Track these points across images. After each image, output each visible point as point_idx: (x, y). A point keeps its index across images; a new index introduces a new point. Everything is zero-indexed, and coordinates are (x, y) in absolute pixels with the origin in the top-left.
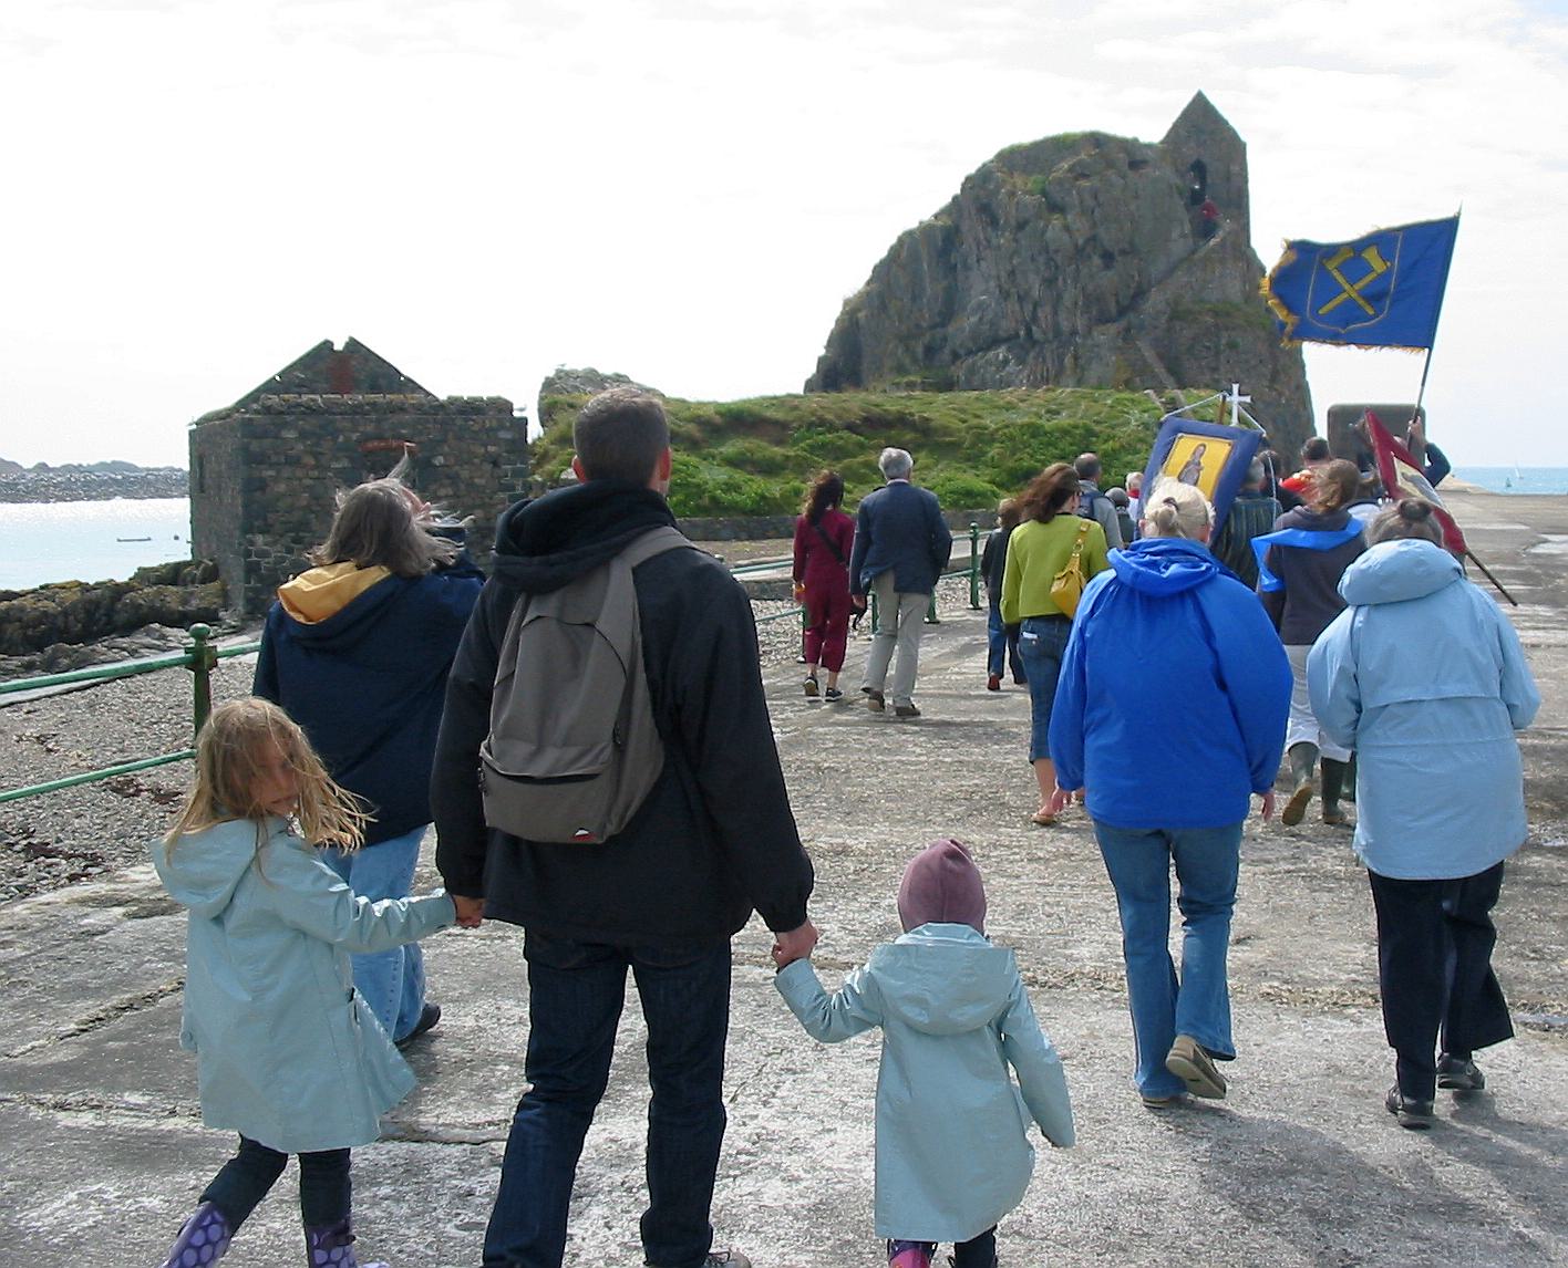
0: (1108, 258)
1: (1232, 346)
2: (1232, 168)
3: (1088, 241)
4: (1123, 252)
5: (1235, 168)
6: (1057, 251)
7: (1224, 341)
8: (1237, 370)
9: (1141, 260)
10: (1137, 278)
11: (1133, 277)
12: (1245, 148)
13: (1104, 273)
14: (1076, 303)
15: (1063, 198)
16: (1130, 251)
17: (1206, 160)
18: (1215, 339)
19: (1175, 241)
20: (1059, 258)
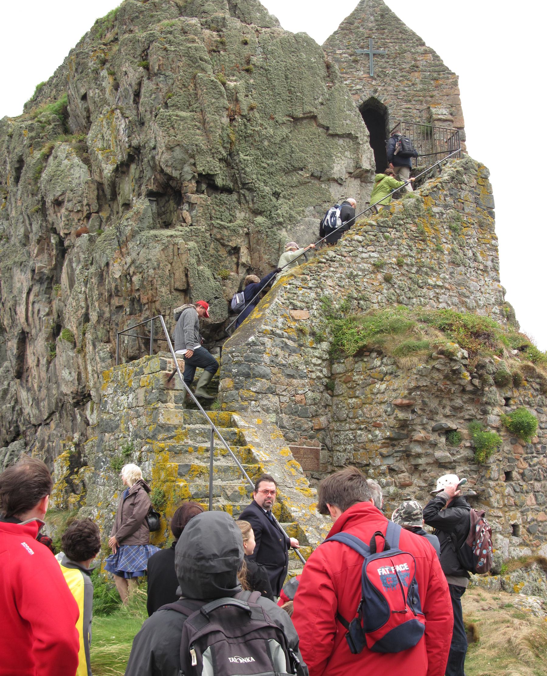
0: (168, 194)
1: (519, 431)
2: (433, 110)
3: (122, 169)
4: (206, 181)
5: (441, 111)
6: (58, 203)
7: (494, 416)
8: (530, 500)
9: (257, 212)
10: (245, 257)
11: (236, 250)
12: (455, 84)
13: (152, 232)
14: (86, 318)
15: (84, 97)
16: (227, 185)
17: (384, 99)
18: (472, 410)
19: (339, 182)
20: (59, 219)
